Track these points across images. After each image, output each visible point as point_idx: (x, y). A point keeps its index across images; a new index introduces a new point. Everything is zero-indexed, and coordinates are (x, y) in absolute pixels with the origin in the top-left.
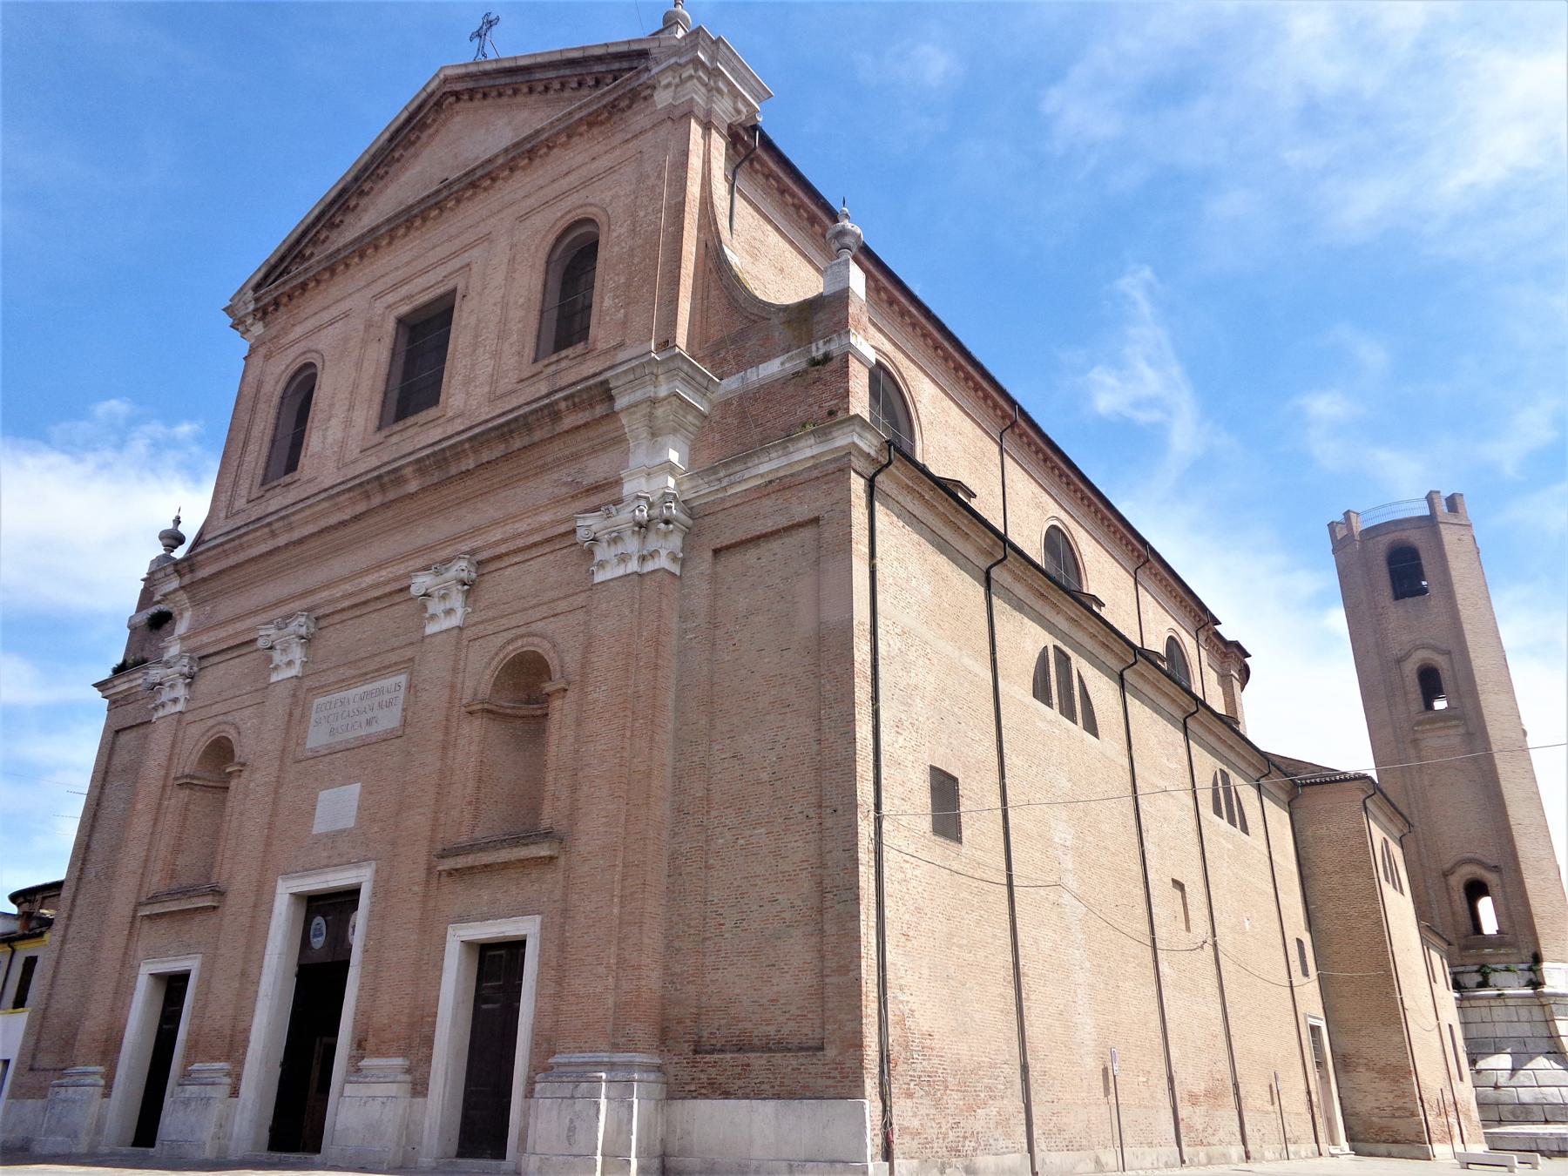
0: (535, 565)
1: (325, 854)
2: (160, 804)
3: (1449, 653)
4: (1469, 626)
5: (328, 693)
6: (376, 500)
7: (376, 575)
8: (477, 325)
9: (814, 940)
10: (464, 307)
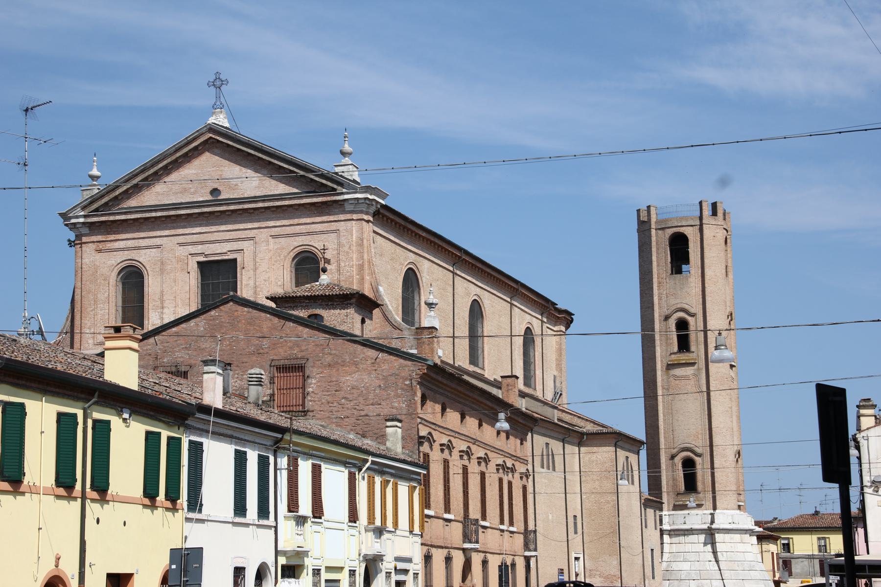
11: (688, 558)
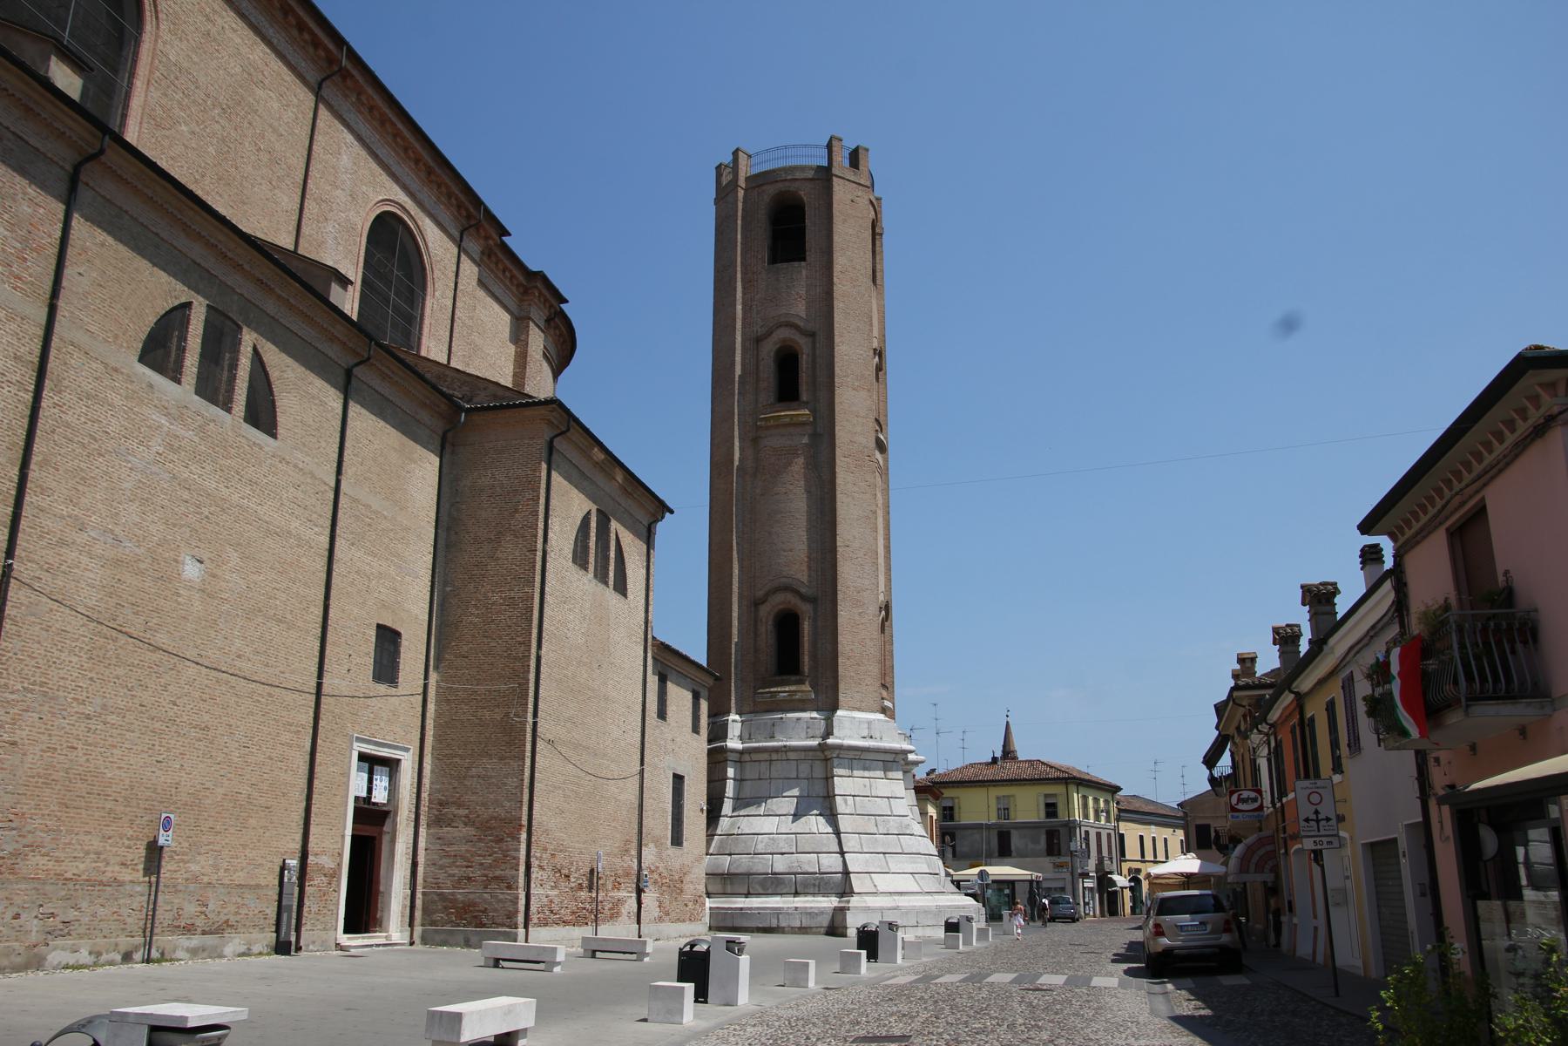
3: (812, 335)
4: (841, 305)
11: (774, 808)
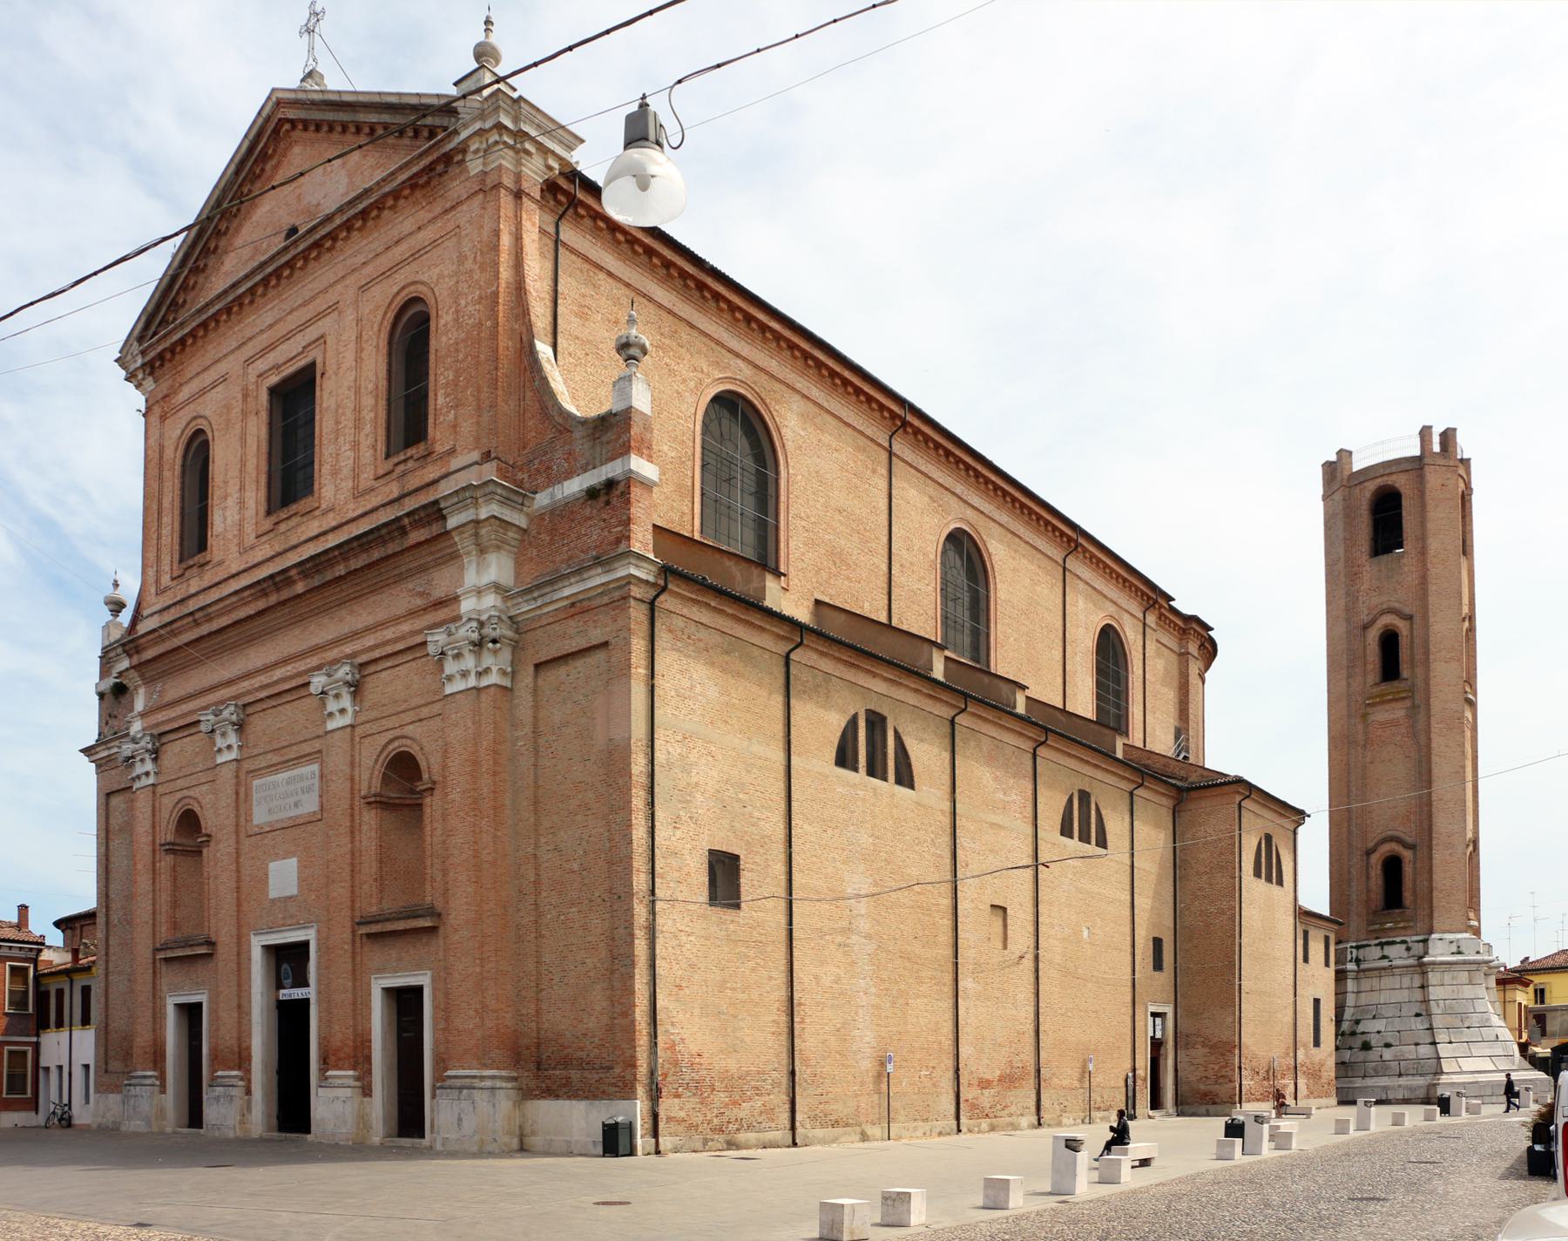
0: (402, 670)
1: (280, 916)
2: (154, 863)
5: (261, 776)
6: (273, 599)
7: (283, 670)
8: (337, 410)
9: (609, 992)
10: (324, 386)
